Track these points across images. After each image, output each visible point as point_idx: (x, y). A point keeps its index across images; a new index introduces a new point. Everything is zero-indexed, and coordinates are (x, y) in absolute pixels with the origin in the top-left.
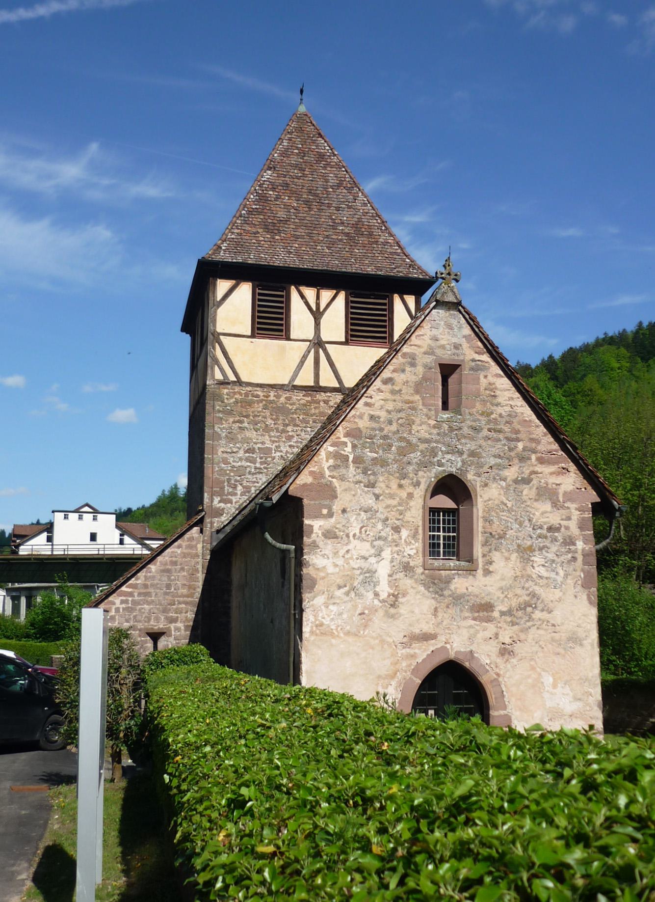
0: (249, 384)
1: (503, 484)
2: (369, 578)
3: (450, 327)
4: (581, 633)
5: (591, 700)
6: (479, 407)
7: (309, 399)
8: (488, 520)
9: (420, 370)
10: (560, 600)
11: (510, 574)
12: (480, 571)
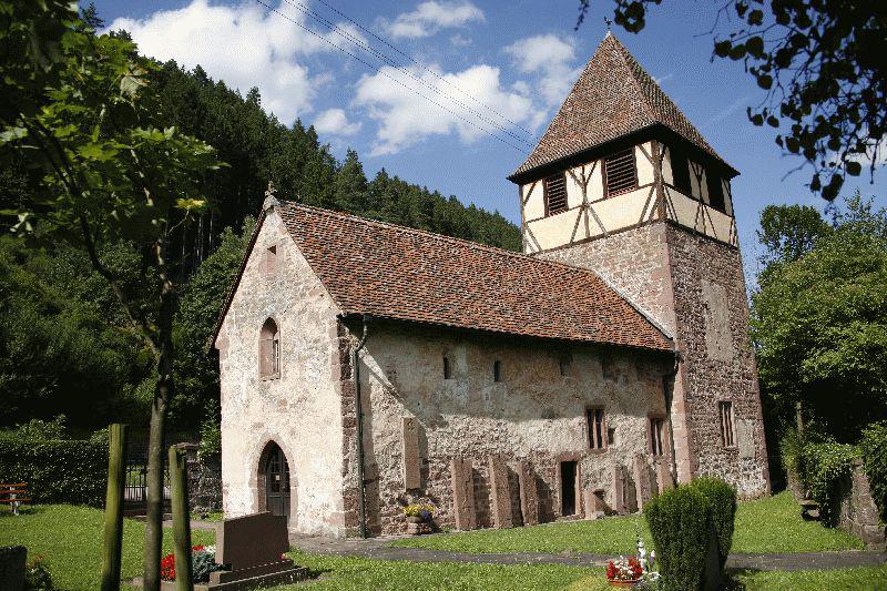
0: (546, 251)
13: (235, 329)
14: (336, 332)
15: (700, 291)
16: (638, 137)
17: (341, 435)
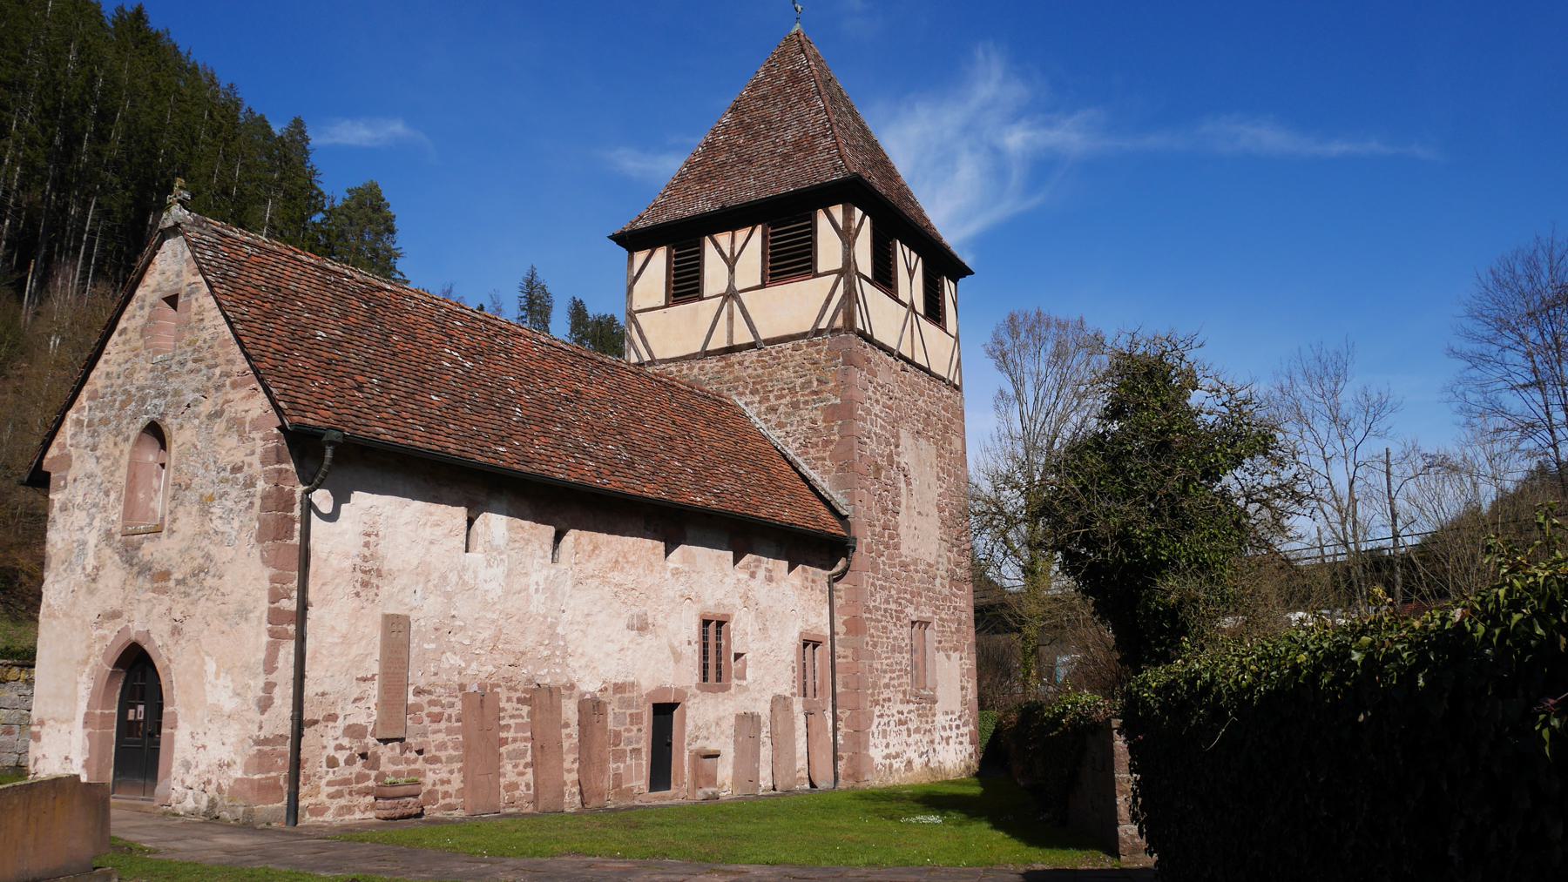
1: (196, 422)
5: (250, 695)
7: (722, 364)
8: (178, 470)
10: (231, 561)
12: (165, 532)
13: (84, 438)
14: (273, 456)
15: (897, 446)
16: (825, 195)
17: (265, 638)
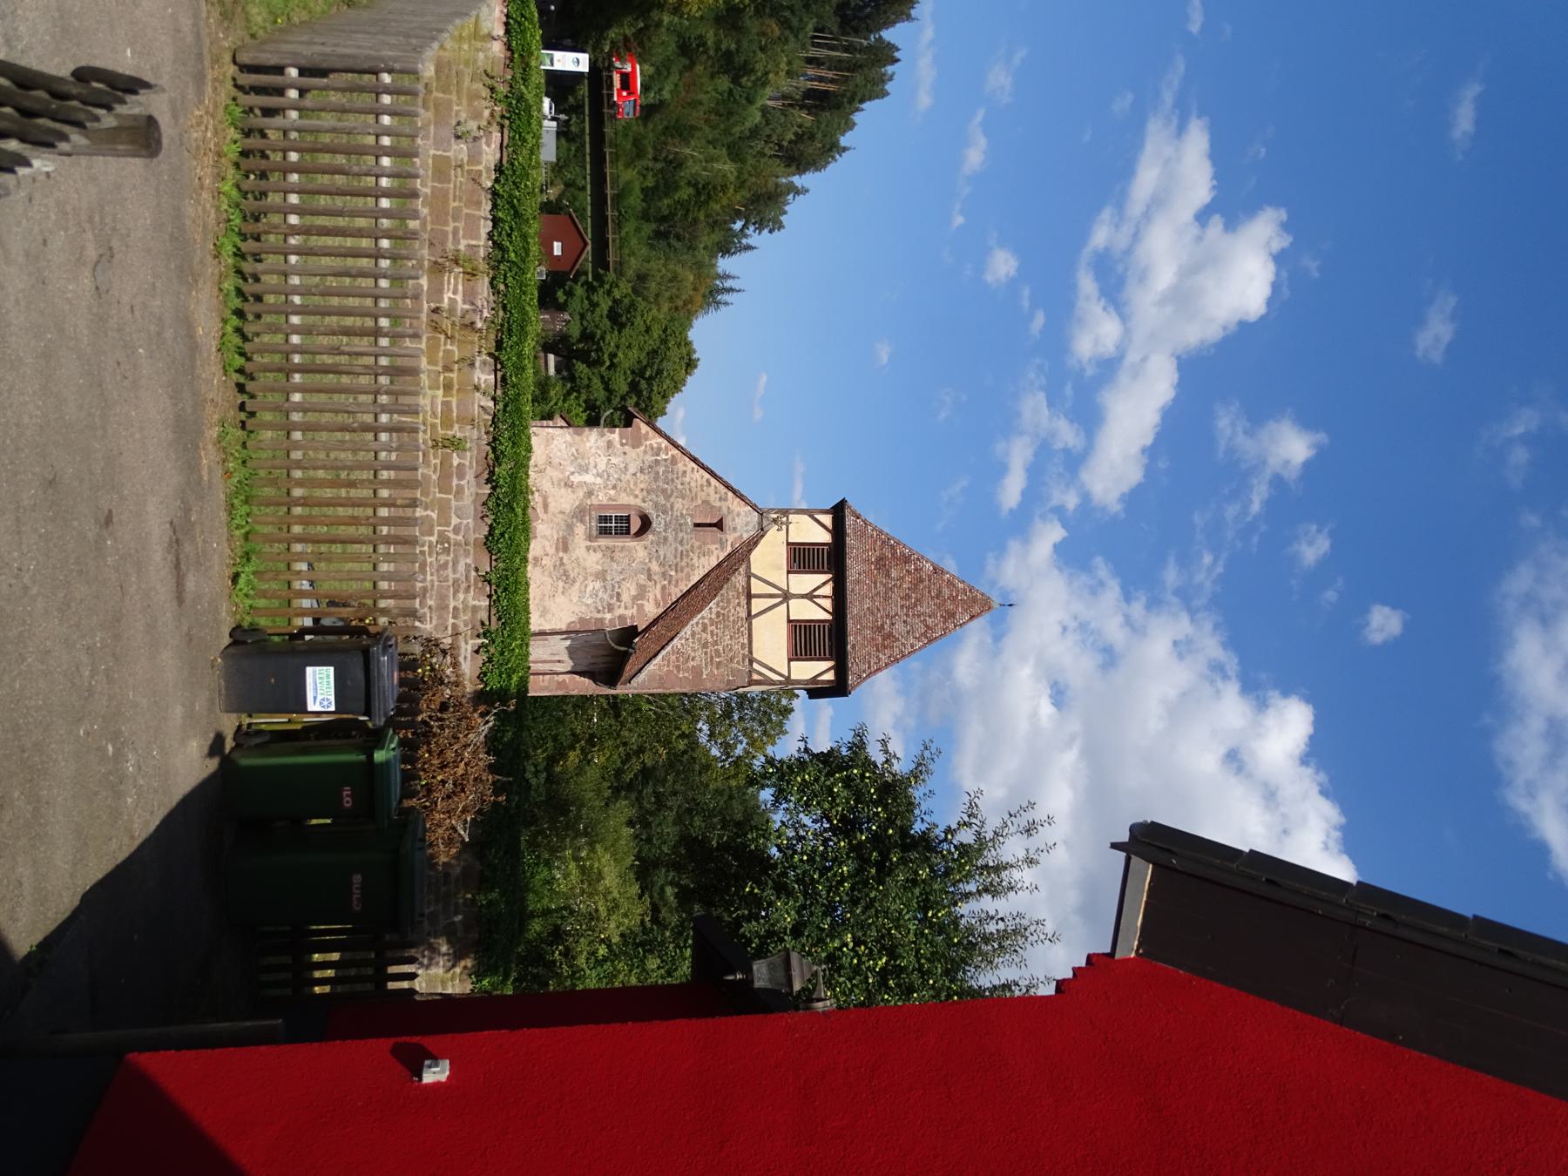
2: (584, 469)
3: (747, 524)
4: (549, 616)
6: (697, 544)
9: (718, 504)
11: (588, 564)
13: (650, 458)
16: (841, 669)
